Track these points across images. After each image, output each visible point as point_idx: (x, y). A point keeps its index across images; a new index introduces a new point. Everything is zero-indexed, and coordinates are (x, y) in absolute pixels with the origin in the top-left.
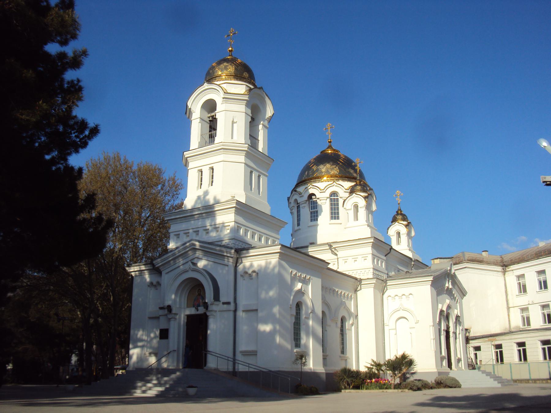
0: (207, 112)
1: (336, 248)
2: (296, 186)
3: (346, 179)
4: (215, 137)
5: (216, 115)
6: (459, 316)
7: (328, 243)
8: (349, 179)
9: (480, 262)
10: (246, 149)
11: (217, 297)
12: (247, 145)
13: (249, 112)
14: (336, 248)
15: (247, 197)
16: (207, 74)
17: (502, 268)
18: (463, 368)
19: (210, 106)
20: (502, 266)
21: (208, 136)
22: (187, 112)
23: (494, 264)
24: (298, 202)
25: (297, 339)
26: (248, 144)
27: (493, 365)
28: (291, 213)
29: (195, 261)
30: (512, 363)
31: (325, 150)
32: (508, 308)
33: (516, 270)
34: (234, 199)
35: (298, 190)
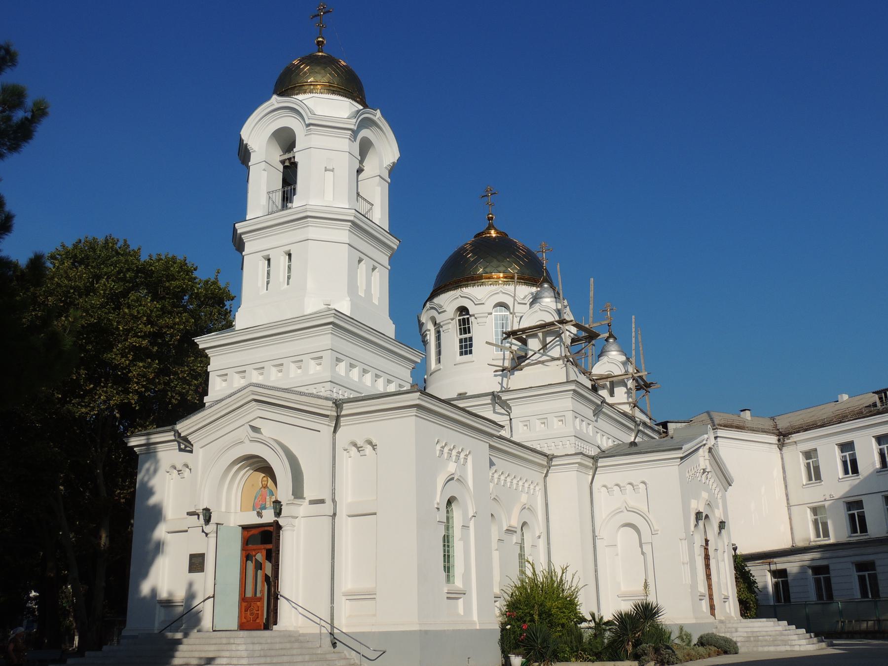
0: (281, 148)
1: (508, 402)
2: (431, 294)
3: (522, 281)
4: (294, 197)
5: (294, 157)
6: (723, 520)
7: (493, 392)
8: (526, 282)
9: (740, 428)
10: (352, 218)
11: (298, 492)
12: (354, 211)
13: (357, 152)
14: (508, 402)
15: (354, 305)
17: (776, 438)
18: (733, 614)
22: (244, 154)
23: (762, 432)
24: (437, 322)
25: (449, 568)
26: (355, 210)
27: (774, 606)
28: (422, 341)
29: (257, 423)
30: (809, 603)
31: (483, 232)
32: (789, 506)
33: (803, 441)
35: (436, 300)
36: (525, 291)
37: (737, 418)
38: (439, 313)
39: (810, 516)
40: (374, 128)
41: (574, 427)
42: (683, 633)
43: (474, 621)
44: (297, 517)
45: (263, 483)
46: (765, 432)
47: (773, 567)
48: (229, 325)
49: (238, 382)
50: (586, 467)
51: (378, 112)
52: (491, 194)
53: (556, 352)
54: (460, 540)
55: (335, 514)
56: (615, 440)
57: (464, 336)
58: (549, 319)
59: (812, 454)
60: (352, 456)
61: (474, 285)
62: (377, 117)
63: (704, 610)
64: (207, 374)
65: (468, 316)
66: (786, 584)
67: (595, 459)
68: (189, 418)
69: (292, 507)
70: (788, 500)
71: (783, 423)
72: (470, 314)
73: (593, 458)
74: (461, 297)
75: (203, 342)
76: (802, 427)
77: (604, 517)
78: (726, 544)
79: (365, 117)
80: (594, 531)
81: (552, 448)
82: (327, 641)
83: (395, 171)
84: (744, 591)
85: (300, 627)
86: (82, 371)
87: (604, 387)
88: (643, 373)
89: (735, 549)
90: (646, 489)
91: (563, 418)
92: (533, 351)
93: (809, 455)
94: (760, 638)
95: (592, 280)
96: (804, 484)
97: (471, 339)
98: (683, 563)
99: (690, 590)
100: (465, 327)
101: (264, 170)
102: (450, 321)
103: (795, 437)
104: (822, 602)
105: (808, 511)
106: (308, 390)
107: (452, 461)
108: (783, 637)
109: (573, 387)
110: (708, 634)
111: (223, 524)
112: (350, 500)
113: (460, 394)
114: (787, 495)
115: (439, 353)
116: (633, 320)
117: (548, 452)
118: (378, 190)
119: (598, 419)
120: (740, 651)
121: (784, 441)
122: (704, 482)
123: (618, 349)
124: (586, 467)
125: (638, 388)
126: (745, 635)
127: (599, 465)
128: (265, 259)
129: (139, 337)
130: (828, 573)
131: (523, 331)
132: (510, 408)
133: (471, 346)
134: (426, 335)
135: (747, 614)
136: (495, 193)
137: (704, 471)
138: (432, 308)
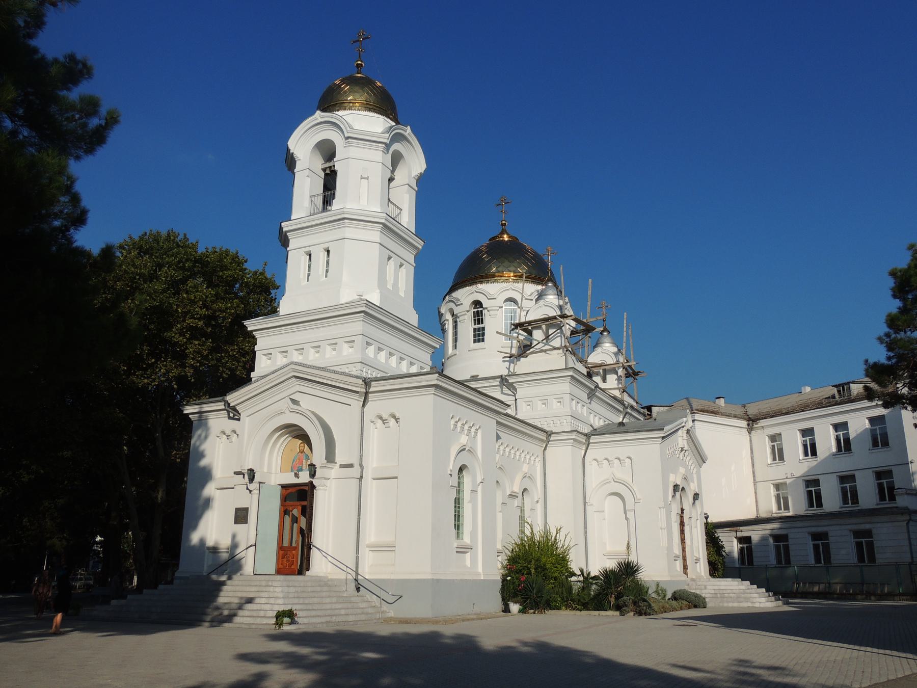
2: (450, 289)
3: (529, 280)
4: (334, 201)
5: (334, 166)
7: (501, 376)
9: (714, 413)
10: (383, 221)
11: (330, 457)
13: (389, 163)
16: (320, 100)
17: (747, 423)
18: (703, 574)
19: (327, 151)
20: (748, 421)
21: (321, 199)
22: (290, 162)
23: (734, 417)
24: (455, 314)
25: (458, 526)
26: (386, 214)
33: (769, 426)
34: (361, 299)
35: (454, 294)
36: (532, 289)
37: (713, 404)
38: (457, 306)
39: (773, 492)
40: (405, 143)
41: (571, 408)
42: (659, 588)
43: (479, 572)
44: (329, 479)
45: (301, 448)
46: (736, 417)
47: (739, 534)
48: (274, 311)
49: (281, 361)
50: (580, 442)
51: (409, 129)
52: (505, 203)
53: (557, 342)
54: (469, 502)
55: (362, 477)
56: (606, 420)
57: (477, 326)
58: (552, 313)
59: (777, 438)
60: (378, 427)
61: (488, 282)
62: (407, 133)
63: (678, 569)
64: (254, 353)
65: (482, 309)
66: (750, 549)
67: (588, 436)
68: (238, 390)
69: (325, 470)
70: (754, 476)
71: (752, 410)
72: (484, 307)
73: (586, 435)
74: (477, 292)
75: (251, 325)
76: (769, 414)
77: (594, 487)
78: (699, 513)
79: (397, 133)
80: (585, 498)
81: (551, 425)
82: (353, 586)
83: (422, 180)
84: (713, 554)
85: (329, 573)
86: (145, 347)
87: (597, 374)
88: (632, 363)
89: (707, 518)
90: (632, 463)
91: (561, 400)
92: (537, 341)
93: (774, 438)
94: (726, 595)
95: (590, 280)
96: (769, 463)
97: (483, 329)
98: (661, 529)
99: (666, 552)
100: (479, 318)
101: (308, 176)
102: (466, 313)
103: (763, 423)
104: (781, 566)
105: (772, 486)
106: (341, 369)
107: (464, 434)
108: (746, 595)
109: (571, 373)
110: (680, 590)
111: (265, 483)
112: (375, 465)
113: (473, 376)
114: (754, 473)
115: (455, 340)
116: (625, 316)
117: (548, 429)
118: (407, 197)
119: (592, 402)
120: (708, 605)
121: (753, 425)
122: (681, 459)
123: (610, 342)
124: (580, 442)
125: (628, 376)
126: (713, 592)
127: (591, 441)
128: (307, 254)
129: (195, 319)
130: (787, 541)
131: (529, 323)
132: (516, 390)
133: (483, 335)
134: (445, 324)
135: (715, 573)
136: (508, 203)
137: (682, 449)
138: (450, 301)
